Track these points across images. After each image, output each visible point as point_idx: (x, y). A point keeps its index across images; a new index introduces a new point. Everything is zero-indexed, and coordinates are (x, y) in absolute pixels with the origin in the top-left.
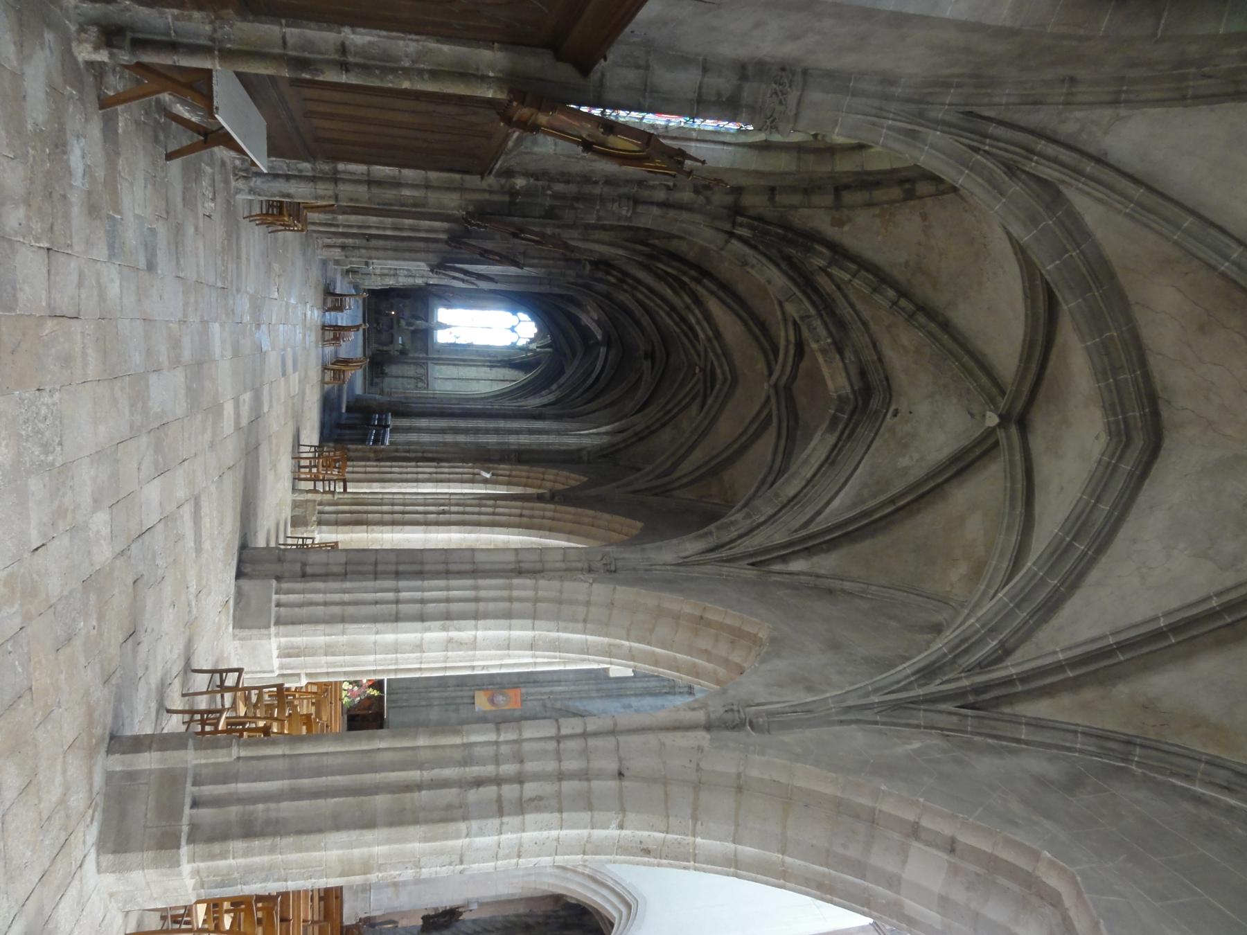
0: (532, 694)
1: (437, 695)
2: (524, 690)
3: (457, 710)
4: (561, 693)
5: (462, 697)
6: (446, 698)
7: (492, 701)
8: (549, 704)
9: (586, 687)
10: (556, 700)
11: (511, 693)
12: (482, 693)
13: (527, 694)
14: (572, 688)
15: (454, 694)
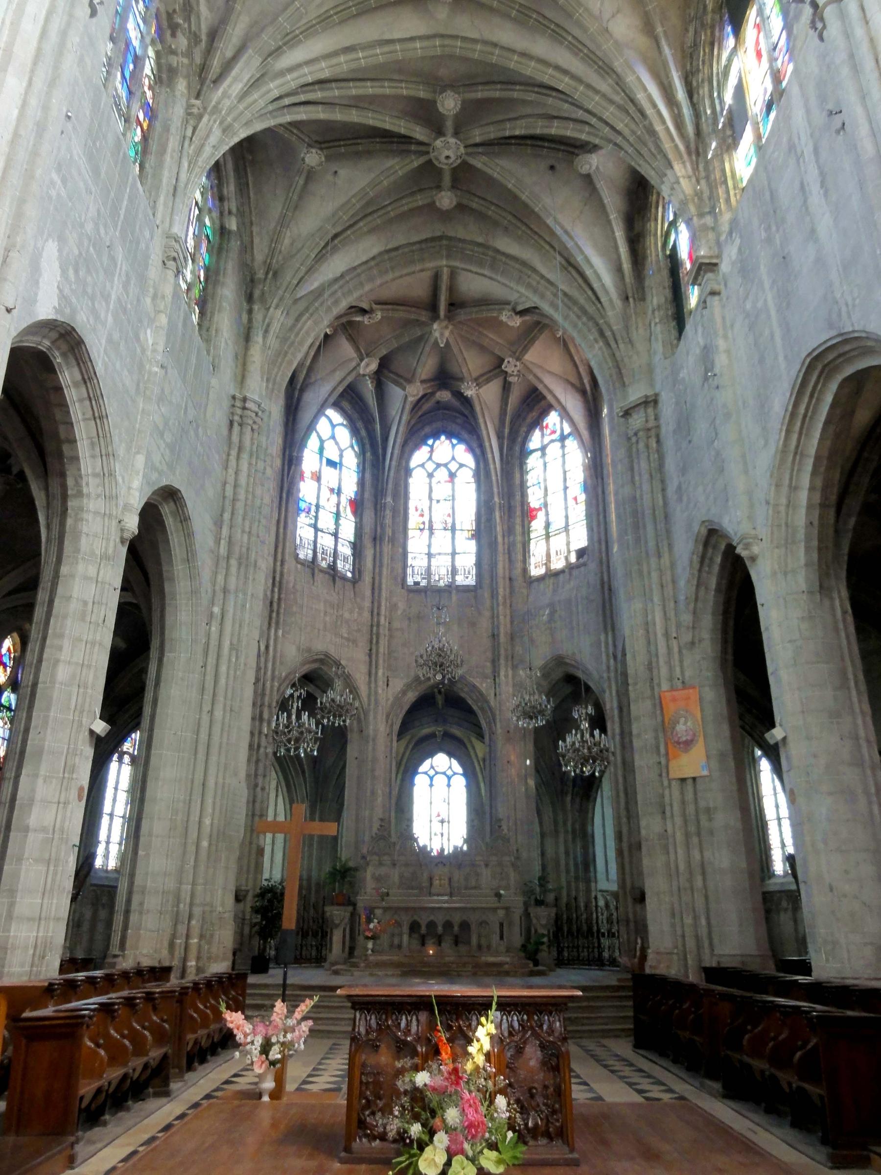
0: (671, 669)
1: (681, 852)
2: (665, 686)
3: (708, 810)
4: (666, 618)
5: (683, 802)
6: (687, 835)
7: (688, 744)
8: (687, 637)
9: (655, 575)
10: (678, 626)
11: (671, 709)
12: (673, 764)
13: (671, 679)
14: (656, 599)
15: (678, 821)
